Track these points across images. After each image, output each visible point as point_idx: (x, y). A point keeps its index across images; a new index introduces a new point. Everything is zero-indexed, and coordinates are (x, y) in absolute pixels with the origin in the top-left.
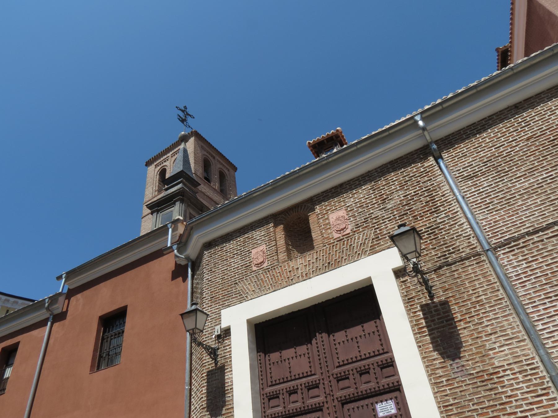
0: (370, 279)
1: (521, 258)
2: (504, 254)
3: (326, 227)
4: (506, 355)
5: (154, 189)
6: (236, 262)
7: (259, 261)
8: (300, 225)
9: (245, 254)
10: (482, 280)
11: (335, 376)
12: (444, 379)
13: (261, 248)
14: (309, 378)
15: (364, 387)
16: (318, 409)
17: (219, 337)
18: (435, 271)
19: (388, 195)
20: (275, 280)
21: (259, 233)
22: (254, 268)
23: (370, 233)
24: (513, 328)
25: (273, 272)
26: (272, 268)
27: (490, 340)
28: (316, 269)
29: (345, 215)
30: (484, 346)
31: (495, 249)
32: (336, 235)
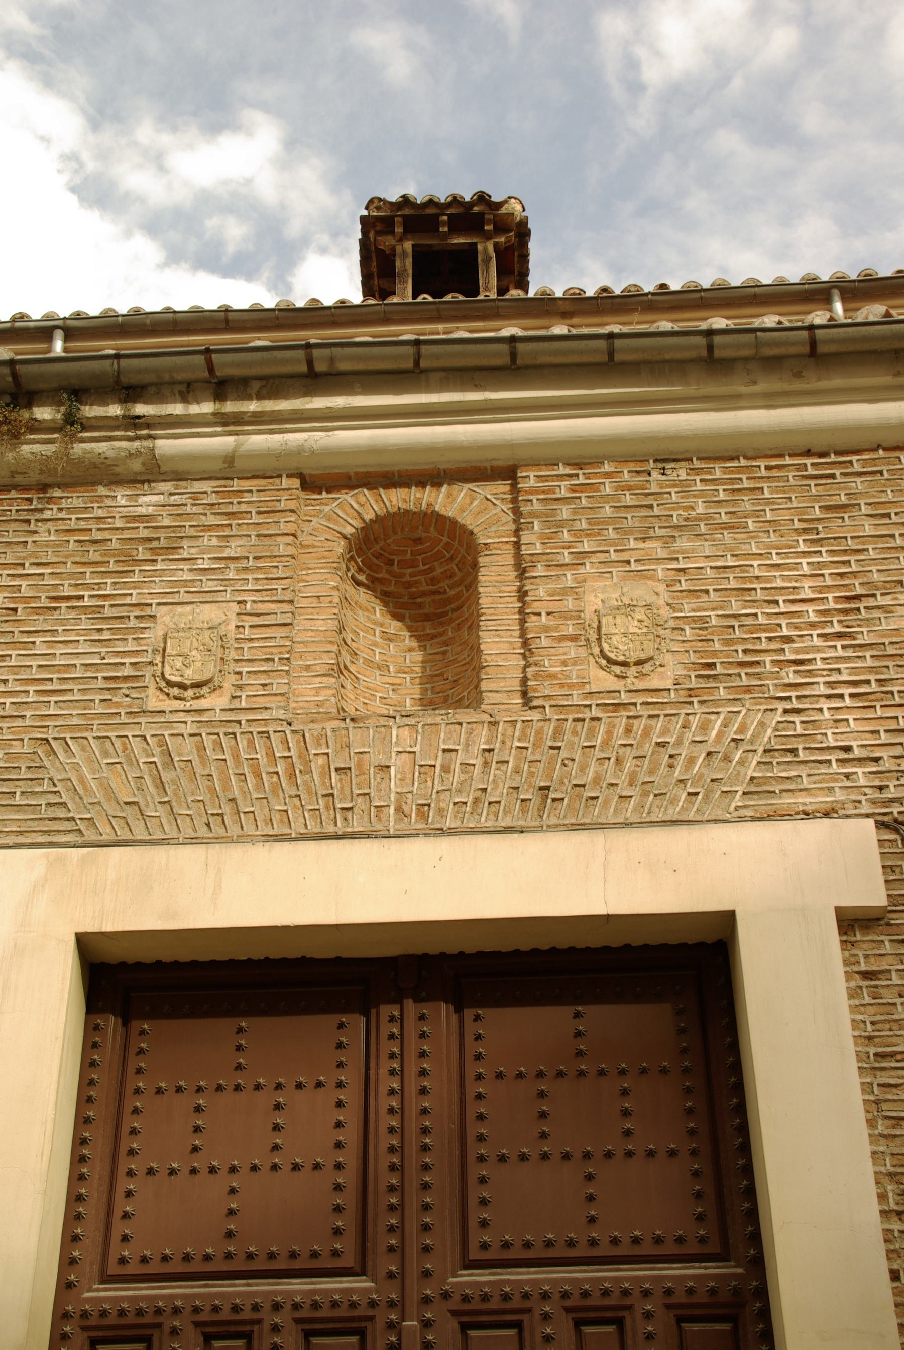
0: (728, 919)
3: (556, 628)
7: (191, 675)
8: (409, 571)
9: (115, 612)
11: (455, 1303)
13: (209, 613)
20: (260, 785)
21: (215, 542)
22: (154, 701)
23: (762, 724)
25: (251, 743)
26: (255, 729)
28: (476, 801)
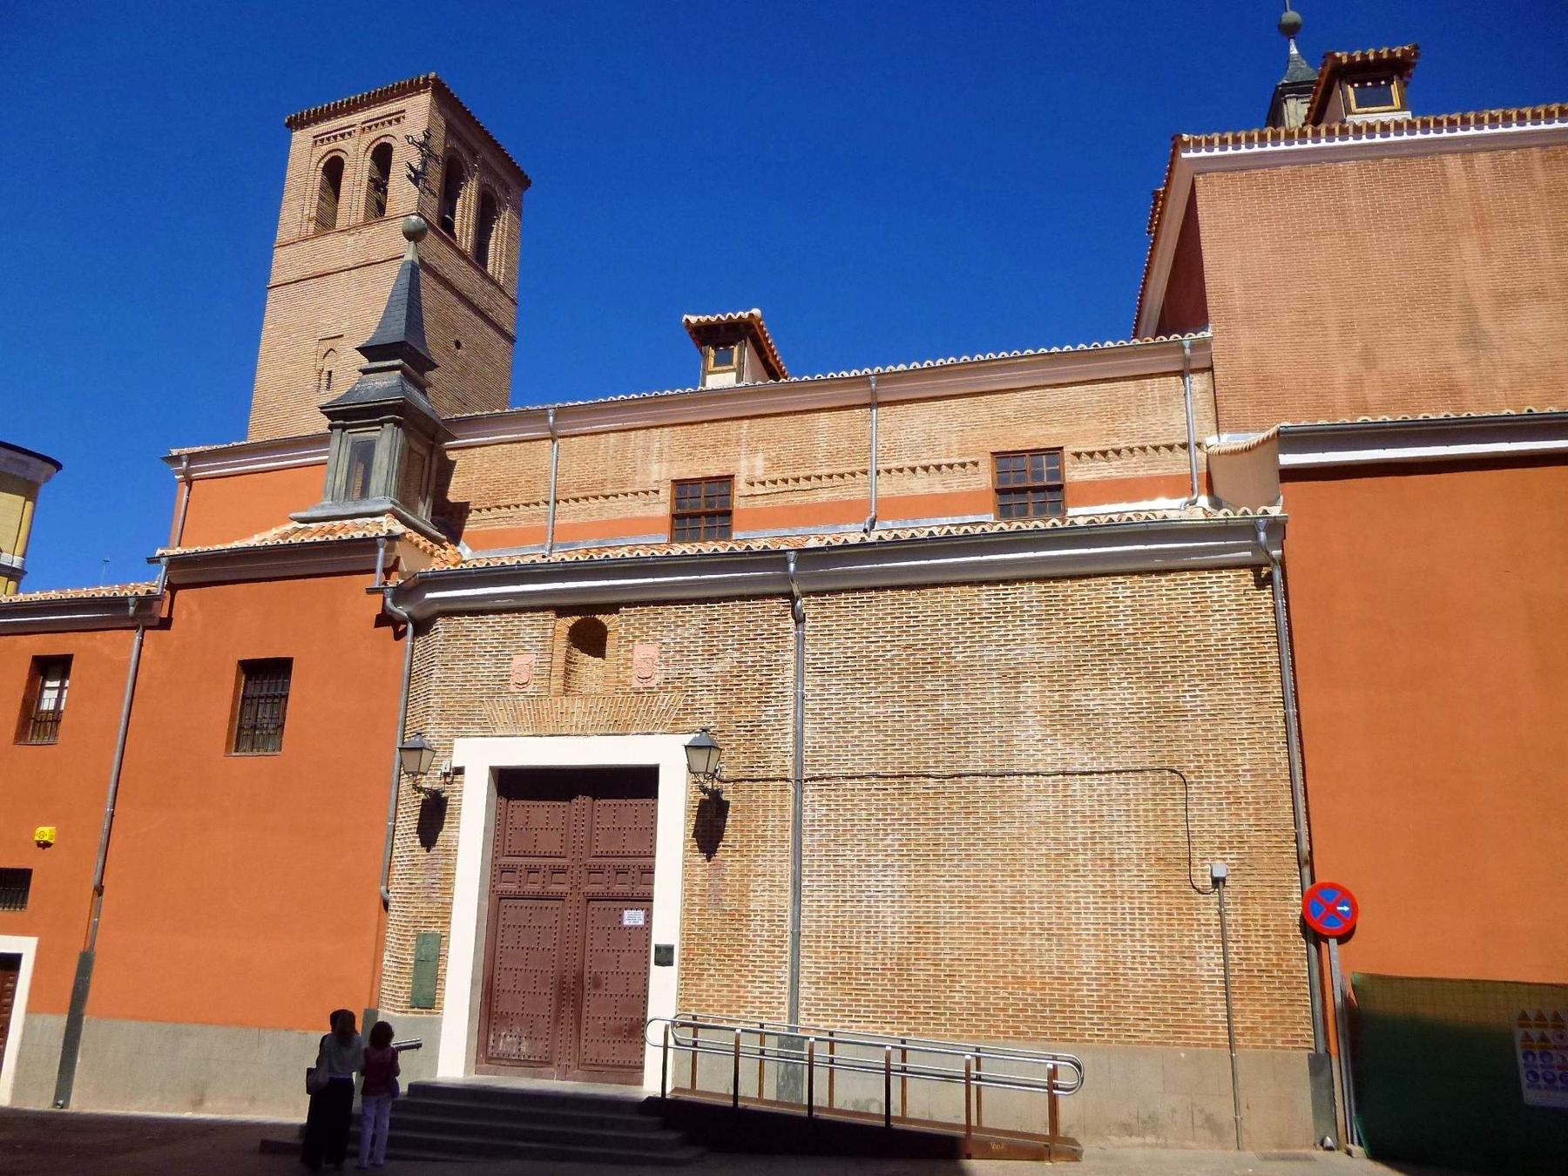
1: (824, 802)
2: (811, 791)
4: (764, 901)
5: (306, 212)
6: (485, 668)
10: (777, 813)
12: (697, 908)
14: (558, 860)
15: (617, 889)
16: (559, 898)
17: (446, 775)
18: (735, 781)
19: (719, 650)
22: (513, 689)
24: (782, 876)
27: (756, 881)
29: (657, 654)
30: (749, 886)
31: (806, 781)
32: (636, 684)
